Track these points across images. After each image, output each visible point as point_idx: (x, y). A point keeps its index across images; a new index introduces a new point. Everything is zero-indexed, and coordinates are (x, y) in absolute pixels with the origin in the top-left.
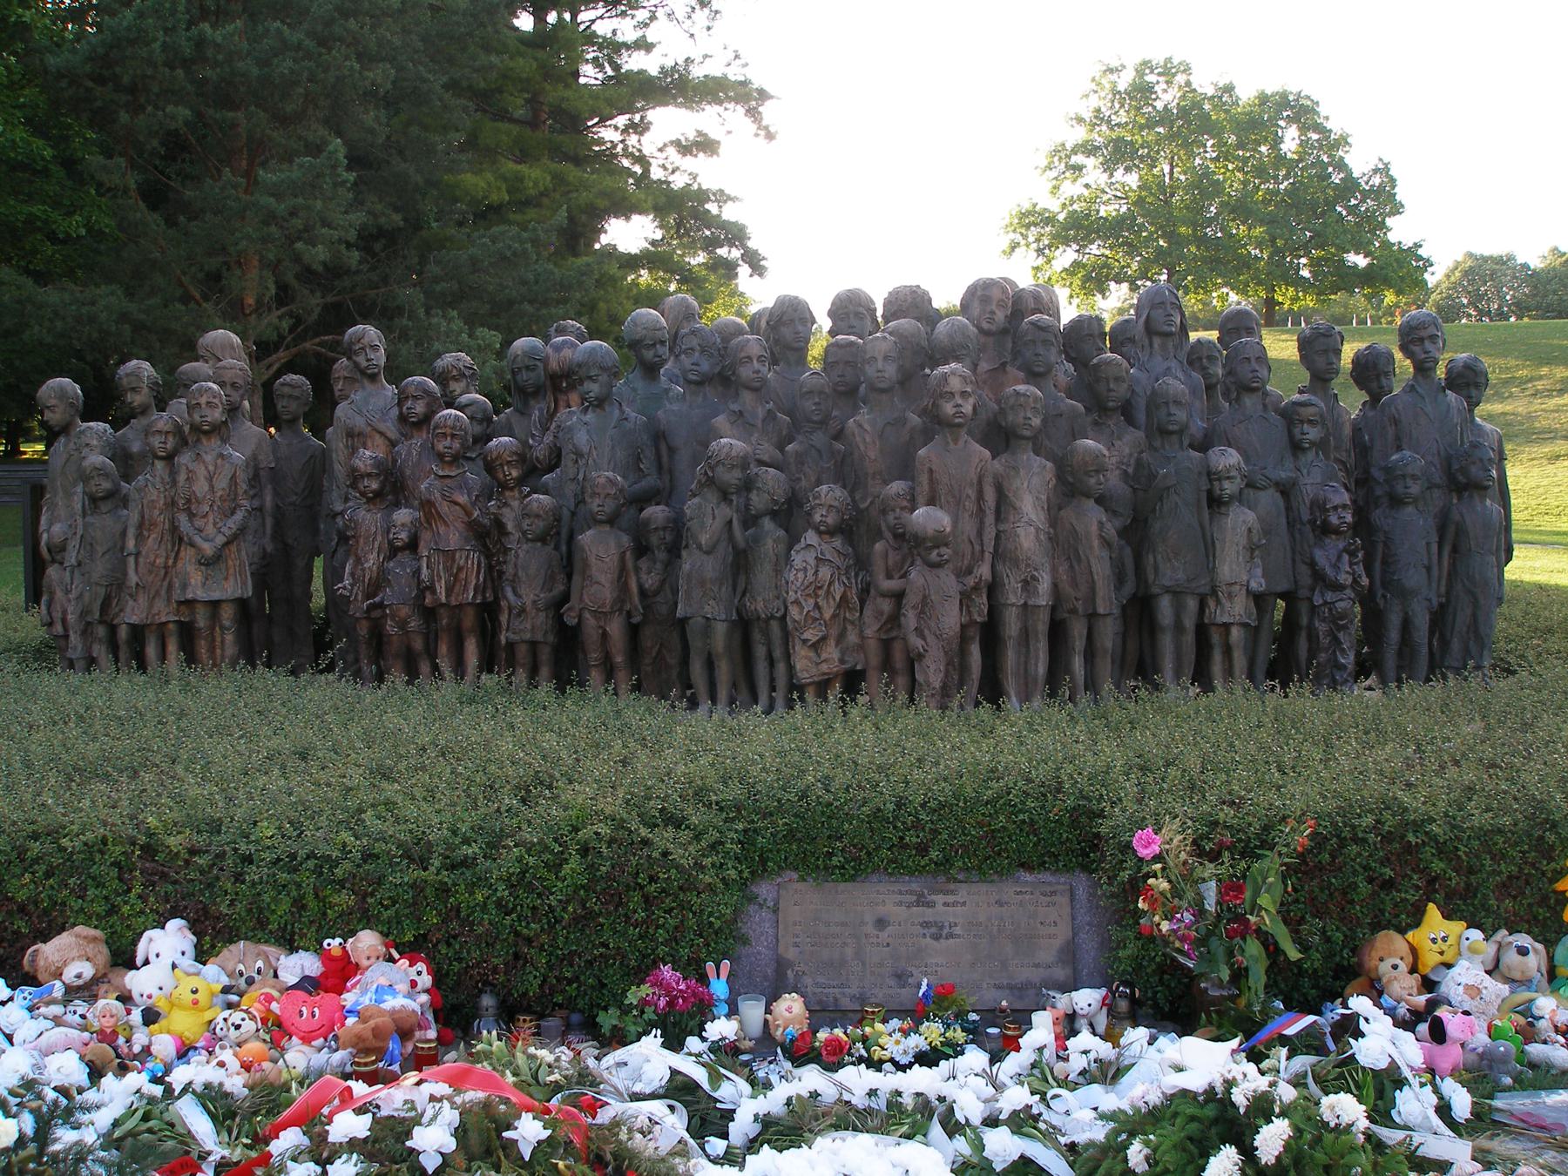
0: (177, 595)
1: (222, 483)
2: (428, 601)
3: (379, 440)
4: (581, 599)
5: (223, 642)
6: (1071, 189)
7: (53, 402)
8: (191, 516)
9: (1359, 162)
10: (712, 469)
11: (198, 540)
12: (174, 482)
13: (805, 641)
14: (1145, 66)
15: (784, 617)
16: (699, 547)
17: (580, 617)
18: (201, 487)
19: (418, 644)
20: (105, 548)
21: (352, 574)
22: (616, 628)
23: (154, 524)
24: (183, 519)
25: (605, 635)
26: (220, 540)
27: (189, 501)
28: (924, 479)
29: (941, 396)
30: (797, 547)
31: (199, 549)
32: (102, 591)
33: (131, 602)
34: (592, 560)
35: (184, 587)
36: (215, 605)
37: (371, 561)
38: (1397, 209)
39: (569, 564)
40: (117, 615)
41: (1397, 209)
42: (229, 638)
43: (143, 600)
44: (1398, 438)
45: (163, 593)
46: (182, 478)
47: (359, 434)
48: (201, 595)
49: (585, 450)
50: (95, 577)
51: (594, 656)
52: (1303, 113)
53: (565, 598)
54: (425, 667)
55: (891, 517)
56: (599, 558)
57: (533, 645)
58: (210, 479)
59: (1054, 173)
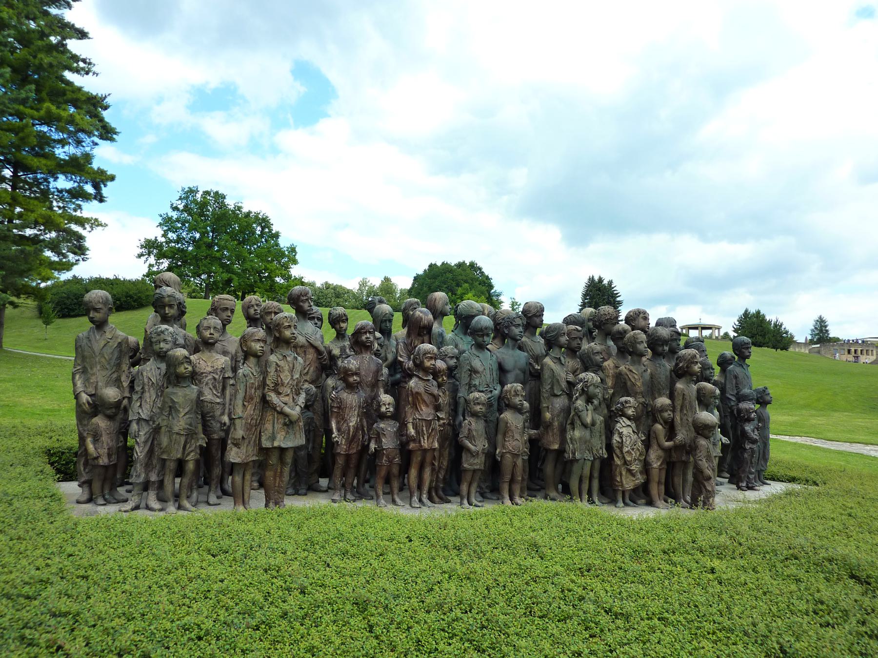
0: (266, 444)
1: (297, 376)
2: (412, 446)
3: (311, 350)
4: (503, 447)
5: (281, 472)
6: (172, 236)
7: (100, 306)
8: (279, 394)
9: (284, 243)
10: (588, 387)
11: (287, 410)
12: (265, 373)
13: (629, 471)
14: (207, 193)
15: (610, 457)
16: (585, 426)
17: (502, 457)
18: (286, 377)
19: (395, 470)
20: (187, 410)
21: (339, 430)
22: (519, 462)
23: (252, 398)
24: (273, 397)
25: (515, 466)
26: (298, 409)
27: (276, 385)
28: (681, 398)
29: (693, 363)
30: (618, 425)
31: (286, 415)
32: (183, 439)
33: (235, 449)
34: (513, 428)
35: (273, 438)
36: (282, 450)
37: (353, 422)
38: (295, 262)
39: (495, 430)
40: (188, 454)
41: (295, 262)
42: (287, 470)
43: (244, 449)
44: (736, 383)
45: (252, 442)
46: (272, 370)
47: (302, 347)
48: (283, 446)
49: (481, 369)
50: (176, 429)
51: (507, 478)
52: (265, 222)
53: (493, 445)
54: (396, 484)
55: (666, 415)
56: (516, 427)
57: (474, 471)
58: (292, 371)
59: (165, 228)
